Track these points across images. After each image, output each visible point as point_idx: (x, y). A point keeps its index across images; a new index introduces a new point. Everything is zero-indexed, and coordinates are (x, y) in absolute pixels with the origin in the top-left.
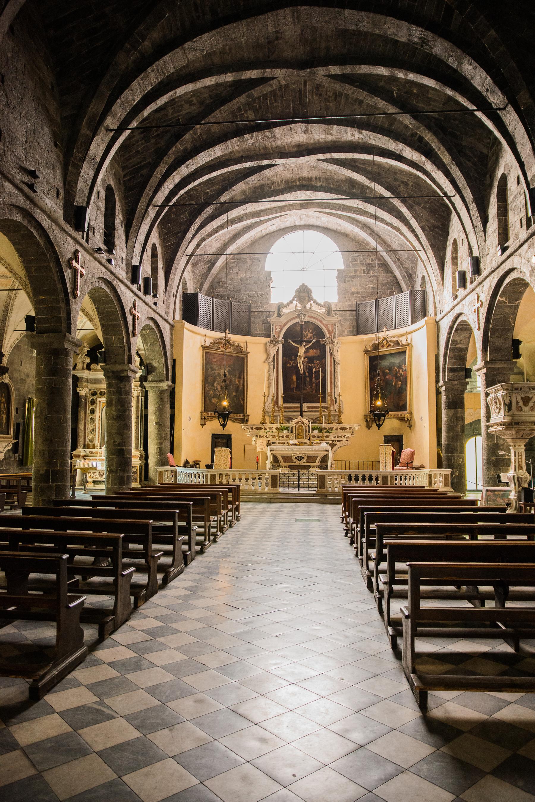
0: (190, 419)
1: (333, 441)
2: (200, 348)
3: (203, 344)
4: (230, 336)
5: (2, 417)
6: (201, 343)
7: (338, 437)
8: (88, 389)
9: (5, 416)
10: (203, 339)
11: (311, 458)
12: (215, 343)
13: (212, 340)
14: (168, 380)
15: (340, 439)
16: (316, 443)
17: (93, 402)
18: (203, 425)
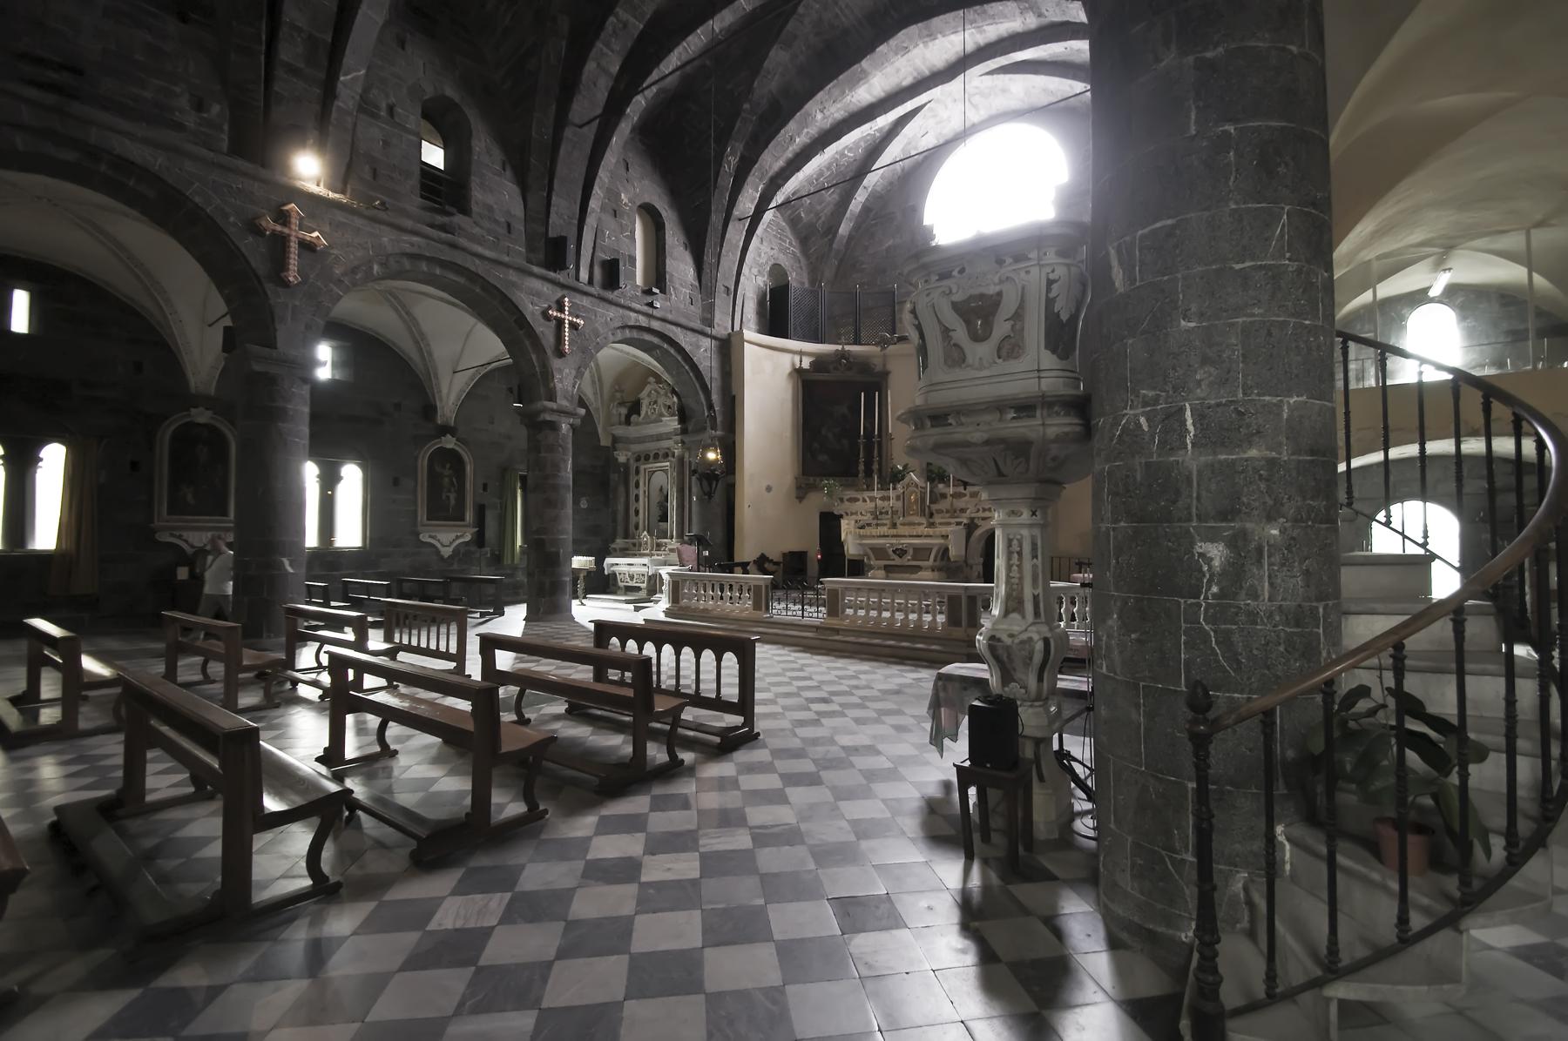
0: (769, 489)
1: (972, 519)
2: (790, 374)
3: (798, 366)
4: (847, 348)
5: (448, 497)
6: (793, 365)
7: (984, 510)
8: (630, 454)
9: (452, 496)
10: (797, 359)
11: (921, 552)
12: (820, 363)
13: (811, 359)
14: (714, 428)
15: (987, 514)
16: (940, 524)
17: (637, 472)
18: (800, 498)
